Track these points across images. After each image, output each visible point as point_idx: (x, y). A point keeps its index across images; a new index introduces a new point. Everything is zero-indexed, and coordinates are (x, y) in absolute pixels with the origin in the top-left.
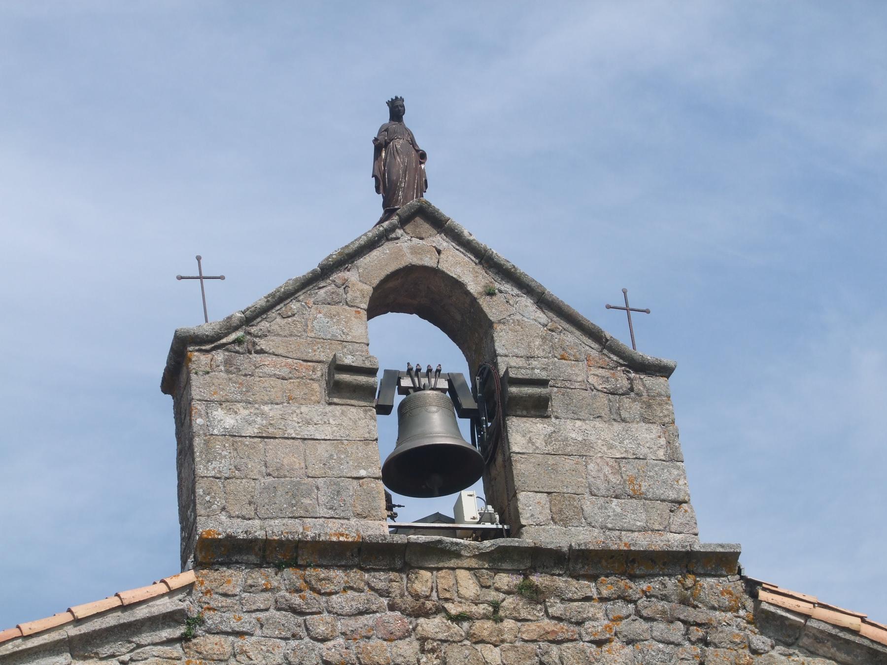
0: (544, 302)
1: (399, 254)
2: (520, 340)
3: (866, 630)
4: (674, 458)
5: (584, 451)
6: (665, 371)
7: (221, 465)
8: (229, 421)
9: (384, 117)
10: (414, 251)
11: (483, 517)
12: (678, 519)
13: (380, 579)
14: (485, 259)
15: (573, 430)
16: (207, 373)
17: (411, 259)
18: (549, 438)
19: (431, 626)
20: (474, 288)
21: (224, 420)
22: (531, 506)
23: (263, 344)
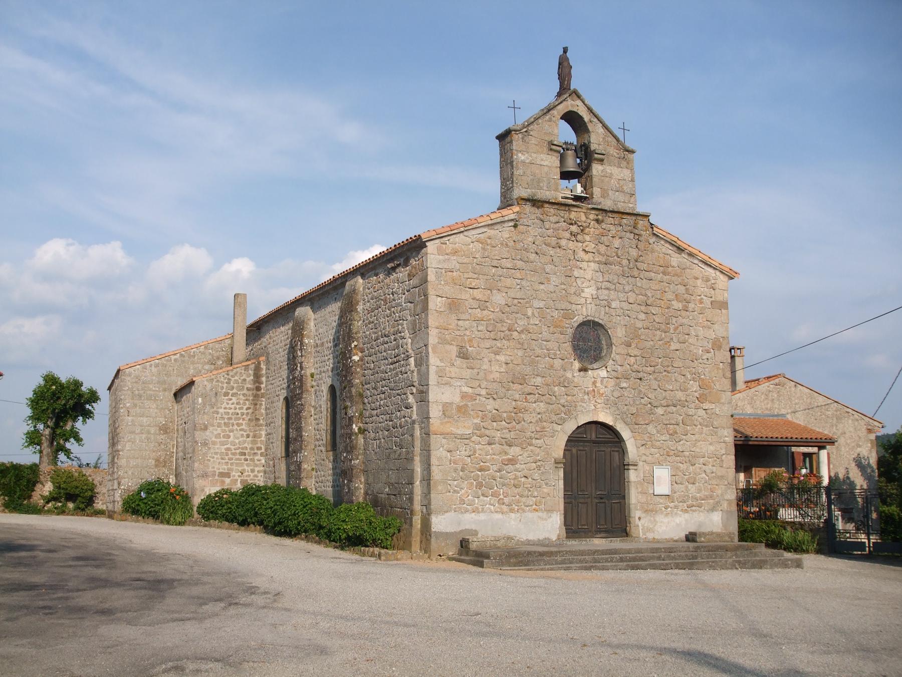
0: (605, 126)
1: (567, 107)
2: (597, 139)
3: (679, 242)
4: (633, 180)
5: (611, 176)
6: (633, 152)
7: (520, 172)
8: (523, 158)
9: (561, 52)
10: (572, 106)
11: (582, 192)
12: (632, 199)
13: (562, 213)
14: (590, 110)
15: (609, 169)
16: (517, 141)
17: (570, 109)
18: (602, 171)
19: (574, 228)
20: (586, 119)
21: (522, 157)
22: (597, 191)
23: (531, 133)
